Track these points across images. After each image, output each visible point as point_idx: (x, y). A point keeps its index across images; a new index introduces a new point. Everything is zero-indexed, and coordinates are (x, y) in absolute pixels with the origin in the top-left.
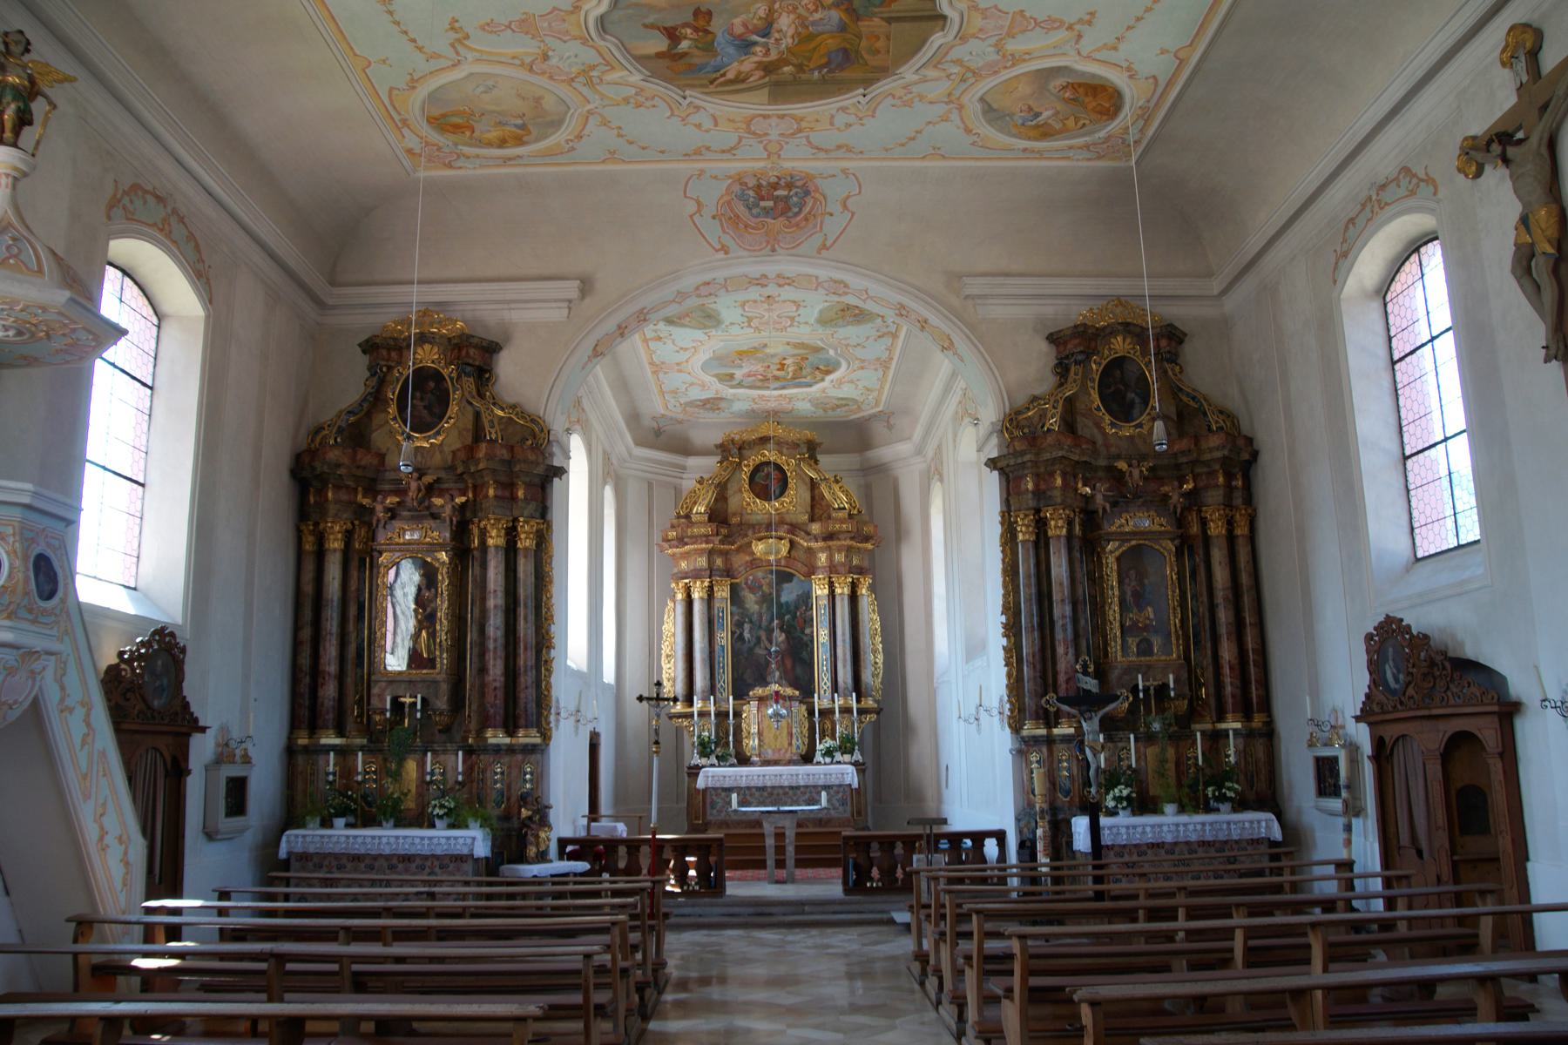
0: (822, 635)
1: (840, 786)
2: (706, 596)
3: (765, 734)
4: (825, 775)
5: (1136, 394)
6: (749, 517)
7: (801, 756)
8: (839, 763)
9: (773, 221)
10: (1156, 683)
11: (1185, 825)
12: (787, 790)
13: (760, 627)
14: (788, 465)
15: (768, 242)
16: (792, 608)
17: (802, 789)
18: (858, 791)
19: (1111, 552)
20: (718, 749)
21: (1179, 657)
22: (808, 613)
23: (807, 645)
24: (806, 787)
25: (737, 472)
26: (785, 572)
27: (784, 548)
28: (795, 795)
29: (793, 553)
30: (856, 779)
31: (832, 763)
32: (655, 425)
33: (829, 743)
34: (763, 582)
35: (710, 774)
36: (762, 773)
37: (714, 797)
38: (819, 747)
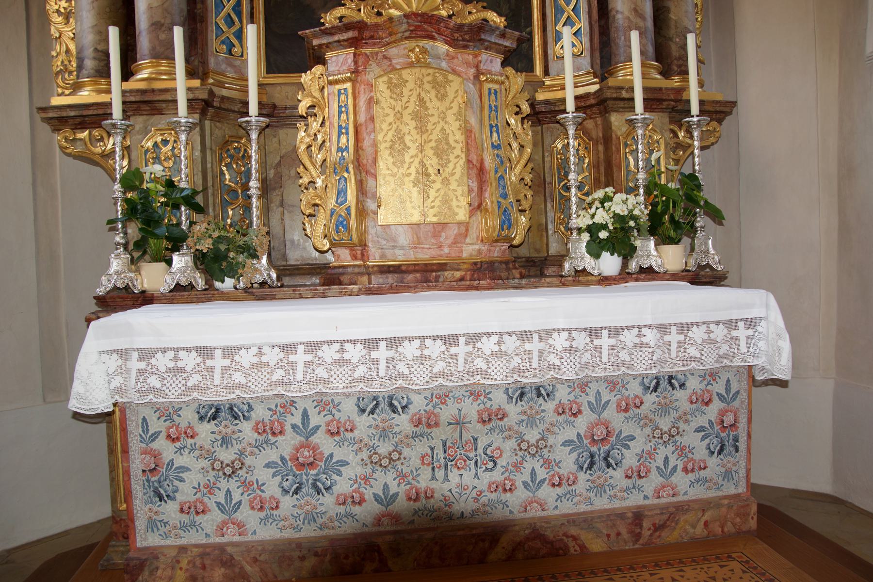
3: (385, 164)
8: (648, 273)
12: (499, 399)
17: (563, 394)
30: (786, 345)
31: (624, 276)
37: (166, 449)
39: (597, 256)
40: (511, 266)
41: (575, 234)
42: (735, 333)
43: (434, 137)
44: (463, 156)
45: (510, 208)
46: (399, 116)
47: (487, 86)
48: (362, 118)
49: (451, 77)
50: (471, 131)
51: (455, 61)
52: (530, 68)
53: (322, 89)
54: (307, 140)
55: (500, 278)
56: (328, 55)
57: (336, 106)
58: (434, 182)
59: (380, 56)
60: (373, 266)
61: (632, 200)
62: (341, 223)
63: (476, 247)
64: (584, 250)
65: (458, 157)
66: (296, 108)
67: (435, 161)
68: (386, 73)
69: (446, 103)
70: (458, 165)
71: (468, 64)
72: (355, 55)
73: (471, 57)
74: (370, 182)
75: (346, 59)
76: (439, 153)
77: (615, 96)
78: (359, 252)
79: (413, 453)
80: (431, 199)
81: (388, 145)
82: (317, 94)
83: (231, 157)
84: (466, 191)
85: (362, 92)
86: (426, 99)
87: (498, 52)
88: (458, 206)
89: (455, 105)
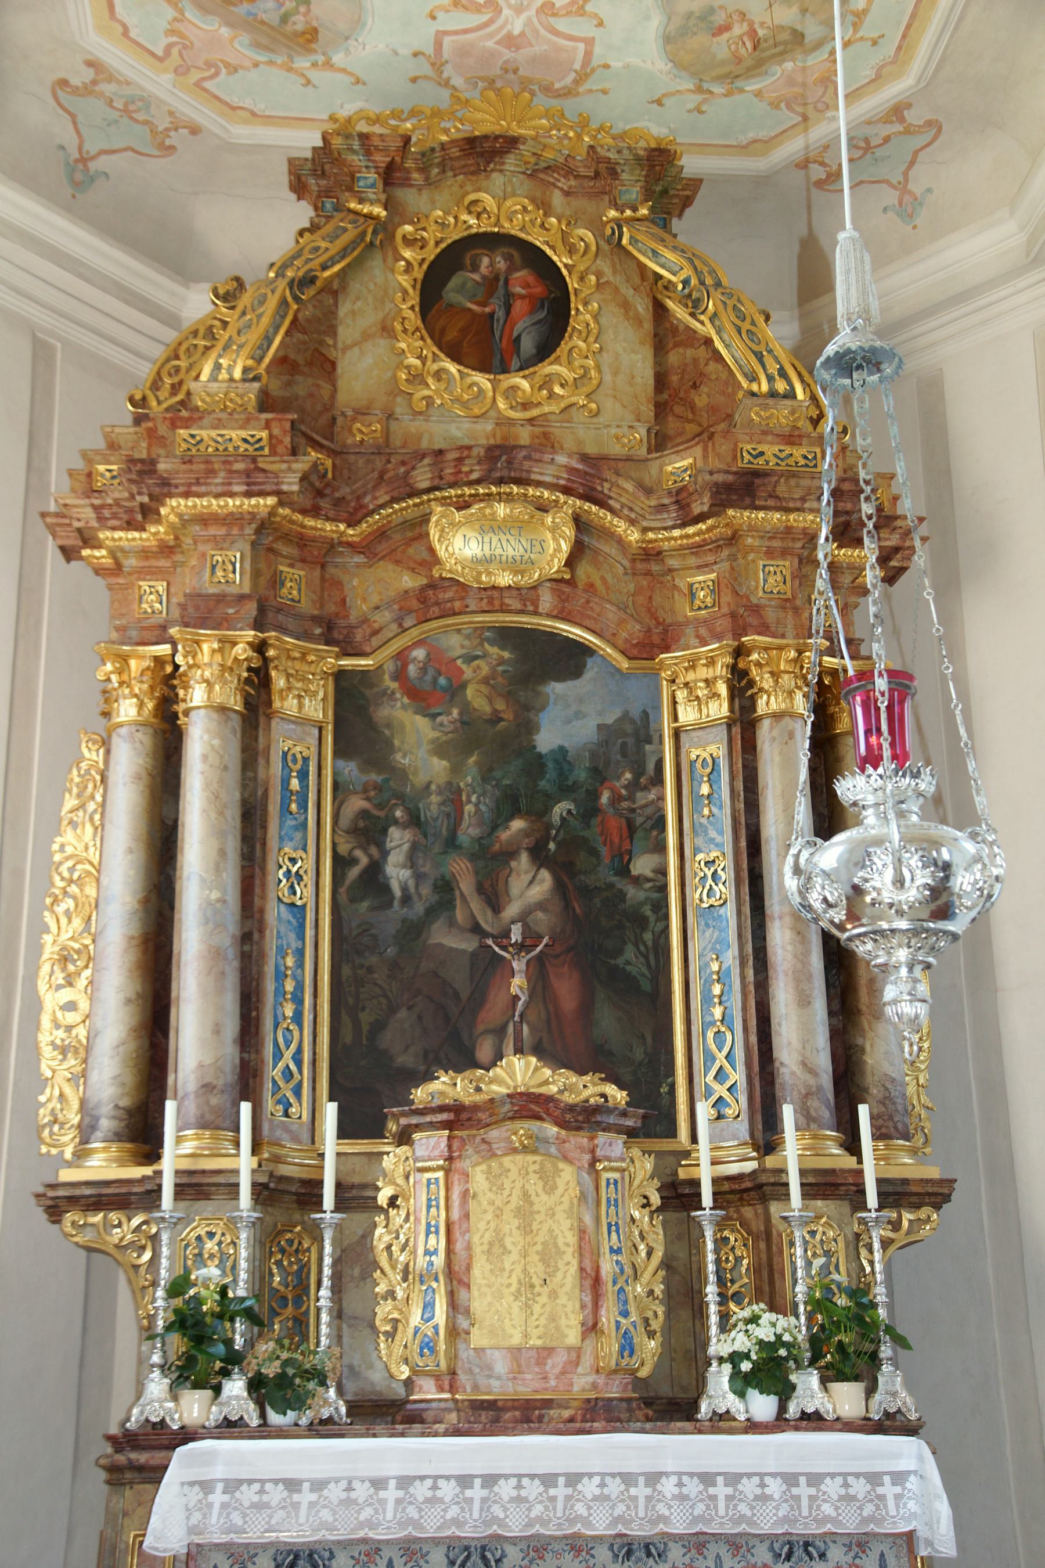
3: (479, 1272)
4: (790, 1479)
6: (415, 426)
8: (813, 1420)
13: (451, 843)
14: (571, 250)
16: (581, 774)
20: (265, 1347)
22: (643, 798)
23: (642, 922)
25: (376, 263)
26: (552, 637)
29: (584, 571)
30: (943, 1508)
31: (780, 1423)
34: (468, 672)
35: (219, 1472)
36: (478, 1468)
39: (741, 1395)
40: (634, 1405)
41: (715, 1364)
42: (880, 1490)
43: (540, 1239)
44: (575, 1263)
45: (632, 1329)
46: (498, 1214)
47: (606, 1175)
48: (455, 1215)
49: (561, 1165)
50: (584, 1232)
51: (567, 1145)
52: (672, 1132)
53: (407, 1177)
54: (387, 1238)
55: (619, 1420)
56: (416, 1136)
57: (424, 1198)
58: (539, 1294)
59: (478, 1139)
60: (463, 1401)
61: (782, 1322)
62: (427, 1344)
63: (590, 1379)
64: (726, 1386)
65: (568, 1263)
66: (375, 1198)
67: (540, 1267)
68: (485, 1159)
69: (554, 1198)
70: (568, 1275)
71: (582, 1149)
72: (449, 1138)
73: (586, 1140)
74: (462, 1294)
75: (438, 1143)
76: (545, 1259)
77: (772, 1180)
78: (447, 1383)
80: (535, 1317)
81: (485, 1247)
82: (400, 1181)
83: (283, 1251)
84: (578, 1306)
85: (456, 1183)
86: (532, 1192)
87: (619, 1132)
88: (568, 1326)
89: (566, 1199)
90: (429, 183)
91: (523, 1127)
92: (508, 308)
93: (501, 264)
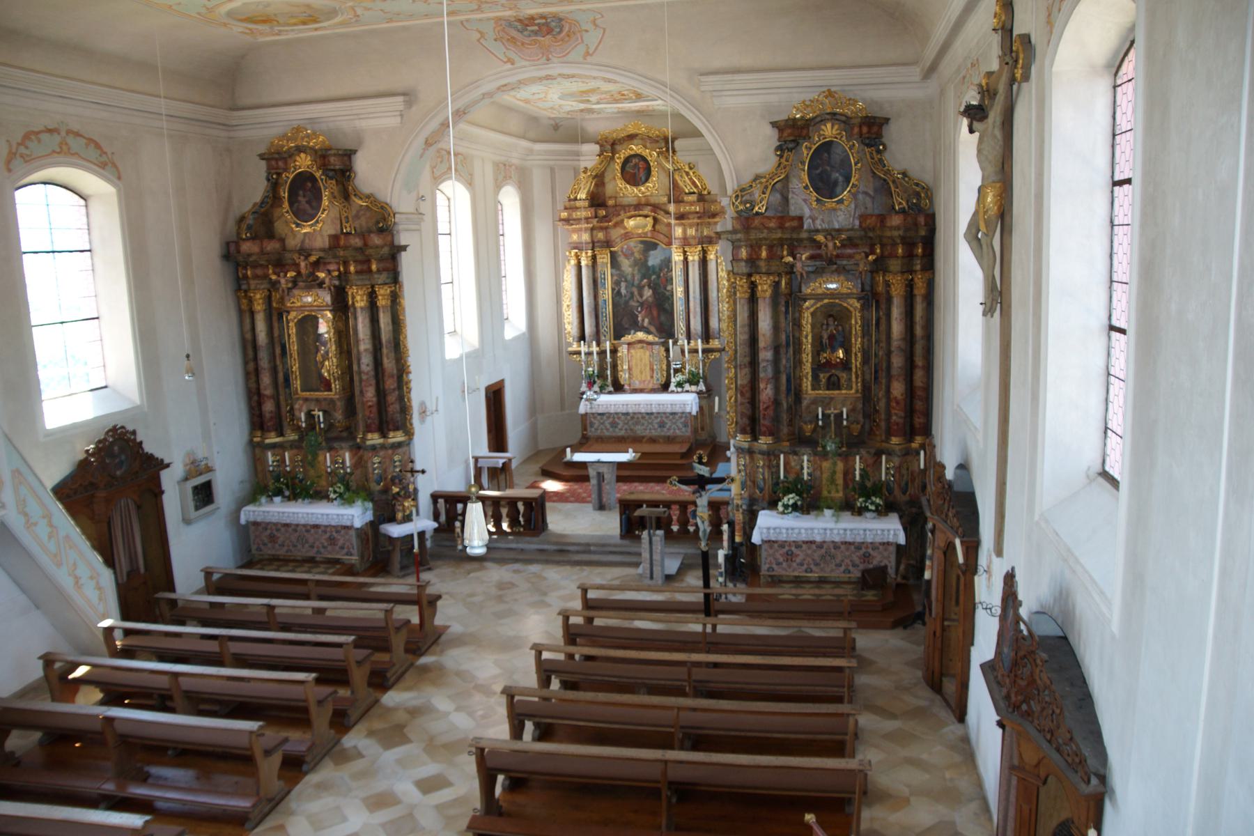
0: (679, 291)
1: (683, 413)
2: (590, 263)
5: (841, 174)
6: (621, 199)
7: (661, 385)
8: (687, 391)
9: (543, 39)
10: (836, 411)
11: (831, 530)
13: (633, 285)
15: (543, 54)
16: (657, 270)
18: (696, 417)
19: (808, 308)
21: (857, 391)
22: (669, 274)
23: (669, 299)
24: (659, 413)
25: (612, 164)
27: (650, 221)
28: (650, 418)
29: (657, 227)
31: (682, 392)
32: (553, 123)
33: (680, 377)
34: (635, 250)
37: (592, 420)
38: (673, 380)
79: (630, 423)
90: (621, 144)
91: (640, 345)
92: (639, 170)
93: (637, 161)
